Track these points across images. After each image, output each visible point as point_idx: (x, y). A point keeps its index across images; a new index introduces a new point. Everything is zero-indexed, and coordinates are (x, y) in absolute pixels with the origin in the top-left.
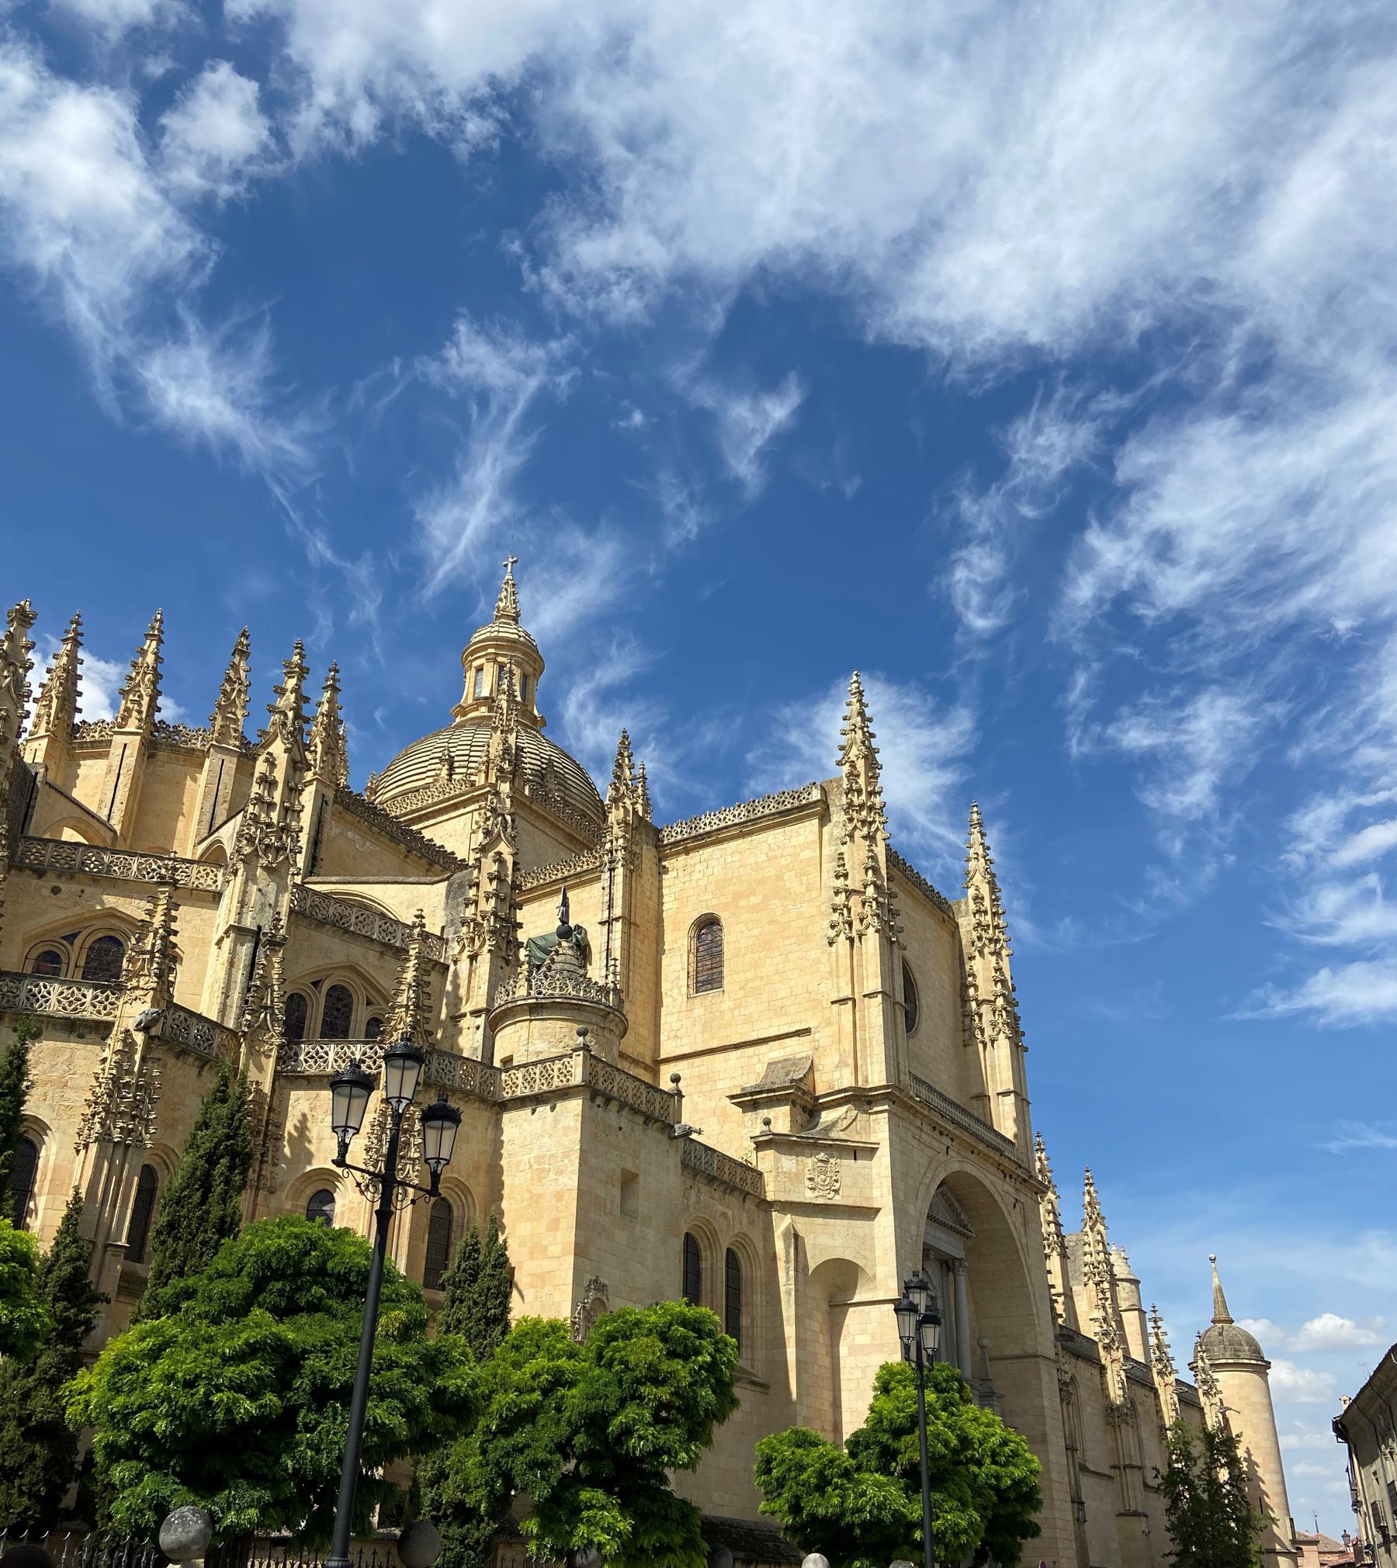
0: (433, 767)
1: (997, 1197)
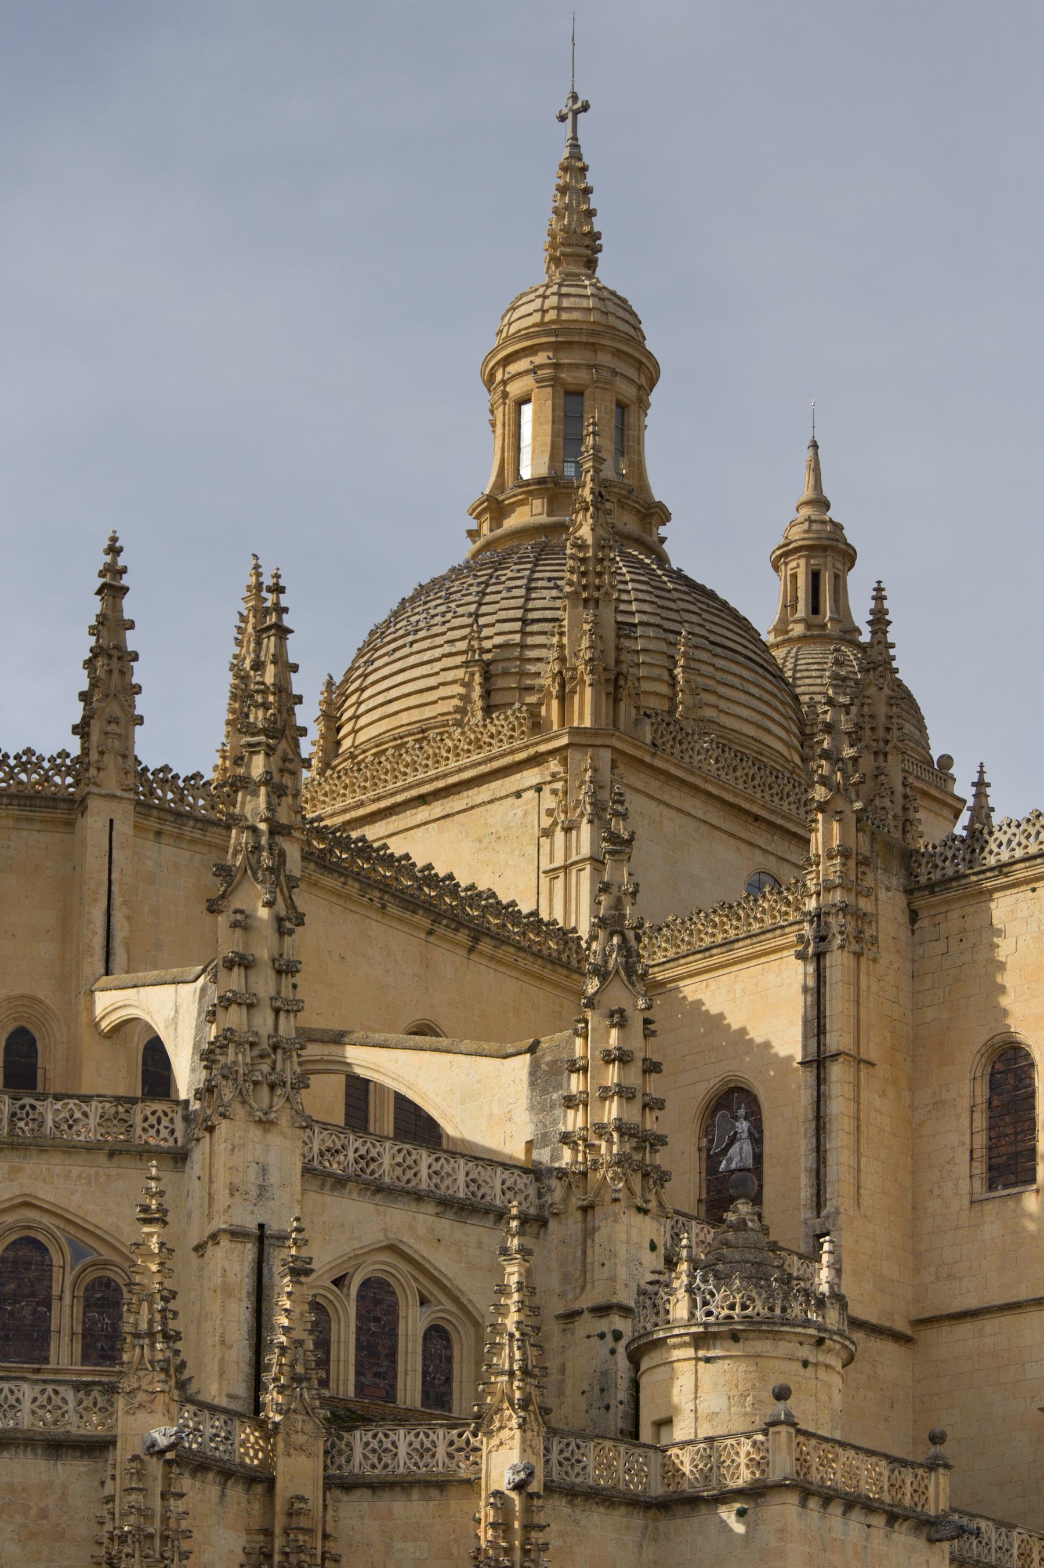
0: (450, 676)
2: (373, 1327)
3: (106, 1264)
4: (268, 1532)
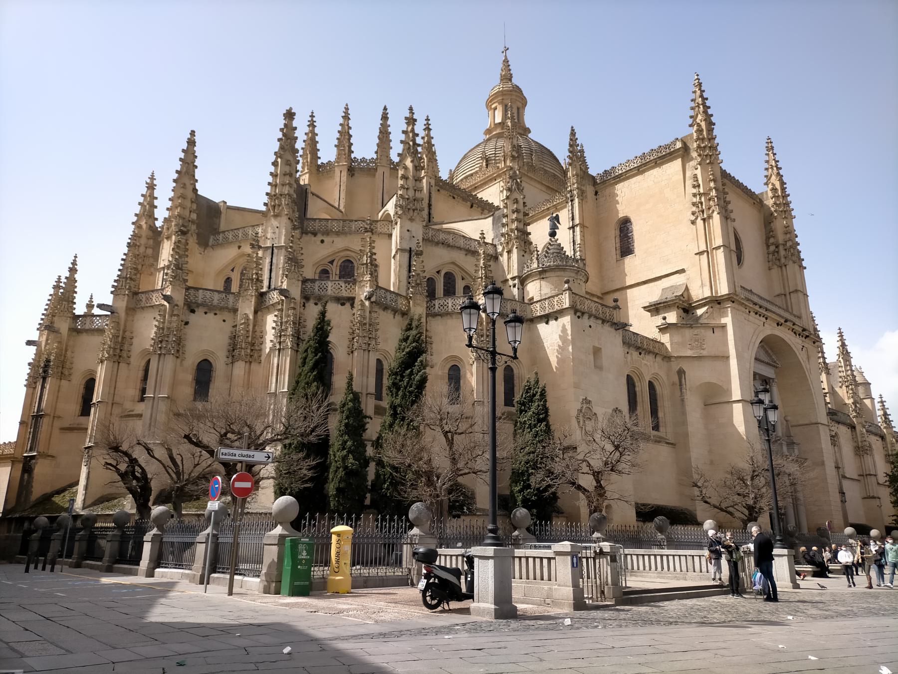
1: (792, 346)
2: (449, 285)
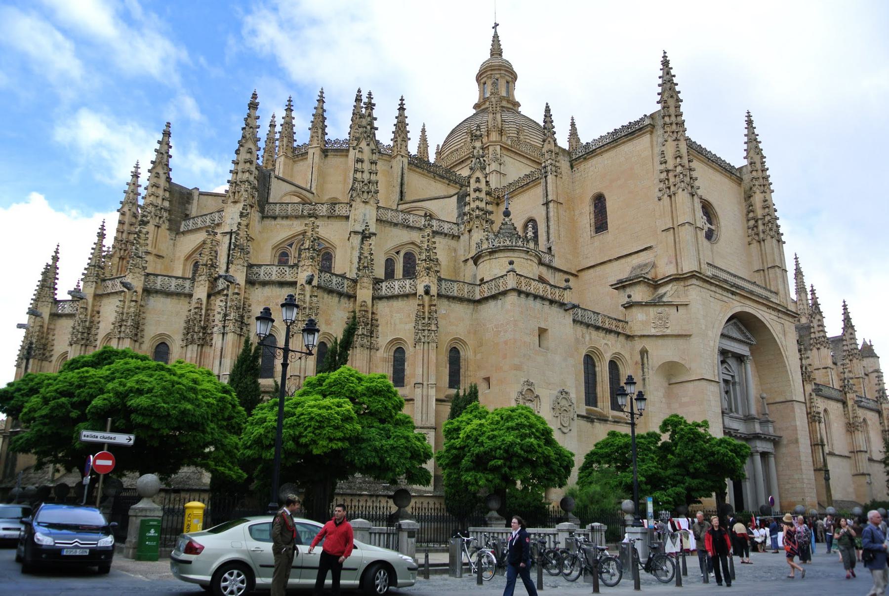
3: (327, 248)
4: (354, 312)
